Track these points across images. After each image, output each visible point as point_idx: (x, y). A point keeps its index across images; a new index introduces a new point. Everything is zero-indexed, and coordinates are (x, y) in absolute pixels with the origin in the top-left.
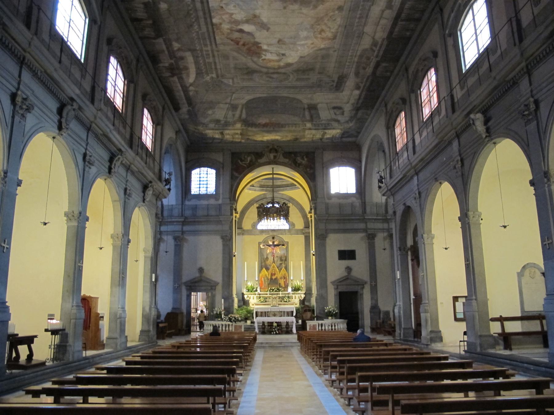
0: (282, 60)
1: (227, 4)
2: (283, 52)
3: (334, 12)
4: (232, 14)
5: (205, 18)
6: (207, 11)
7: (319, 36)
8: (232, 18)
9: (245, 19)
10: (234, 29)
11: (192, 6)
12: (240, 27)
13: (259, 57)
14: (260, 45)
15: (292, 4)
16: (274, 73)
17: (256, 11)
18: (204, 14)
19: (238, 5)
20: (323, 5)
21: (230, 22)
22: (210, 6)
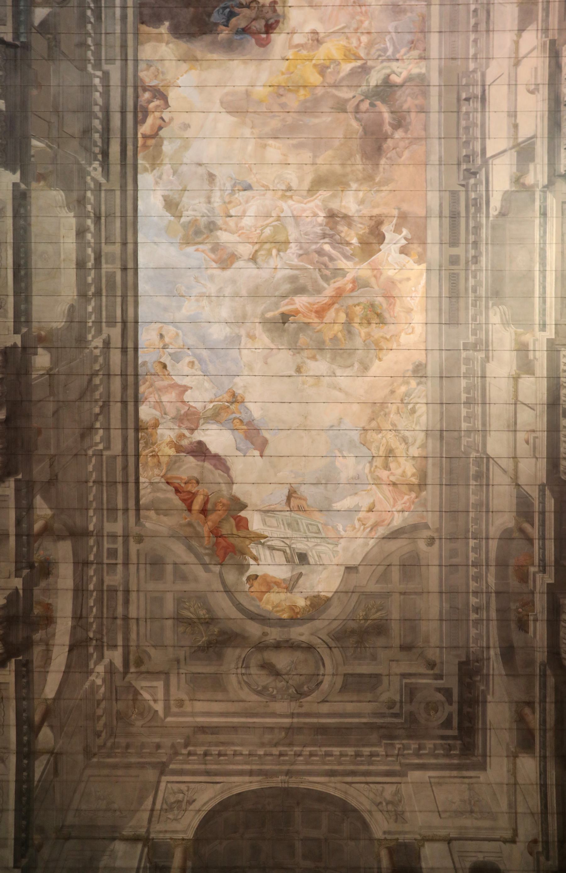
0: (301, 581)
1: (176, 358)
2: (300, 546)
3: (408, 383)
4: (185, 389)
5: (124, 403)
6: (131, 379)
7: (384, 474)
8: (183, 402)
9: (211, 405)
10: (185, 442)
11: (101, 360)
12: (198, 436)
13: (242, 567)
14: (243, 514)
15: (314, 358)
16: (278, 646)
17: (237, 379)
18: (124, 388)
19: (200, 360)
20: (380, 360)
21: (180, 419)
22: (140, 361)
